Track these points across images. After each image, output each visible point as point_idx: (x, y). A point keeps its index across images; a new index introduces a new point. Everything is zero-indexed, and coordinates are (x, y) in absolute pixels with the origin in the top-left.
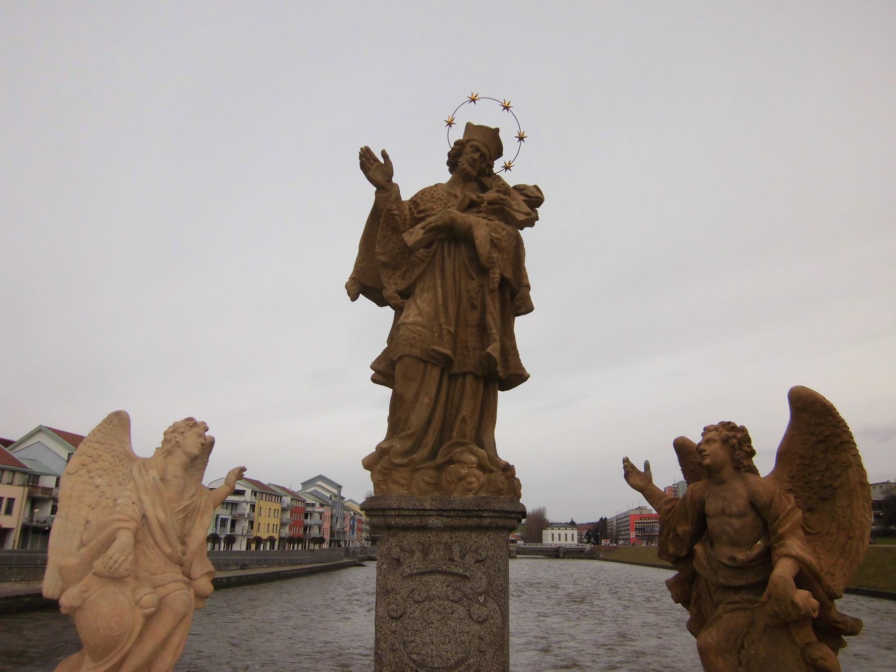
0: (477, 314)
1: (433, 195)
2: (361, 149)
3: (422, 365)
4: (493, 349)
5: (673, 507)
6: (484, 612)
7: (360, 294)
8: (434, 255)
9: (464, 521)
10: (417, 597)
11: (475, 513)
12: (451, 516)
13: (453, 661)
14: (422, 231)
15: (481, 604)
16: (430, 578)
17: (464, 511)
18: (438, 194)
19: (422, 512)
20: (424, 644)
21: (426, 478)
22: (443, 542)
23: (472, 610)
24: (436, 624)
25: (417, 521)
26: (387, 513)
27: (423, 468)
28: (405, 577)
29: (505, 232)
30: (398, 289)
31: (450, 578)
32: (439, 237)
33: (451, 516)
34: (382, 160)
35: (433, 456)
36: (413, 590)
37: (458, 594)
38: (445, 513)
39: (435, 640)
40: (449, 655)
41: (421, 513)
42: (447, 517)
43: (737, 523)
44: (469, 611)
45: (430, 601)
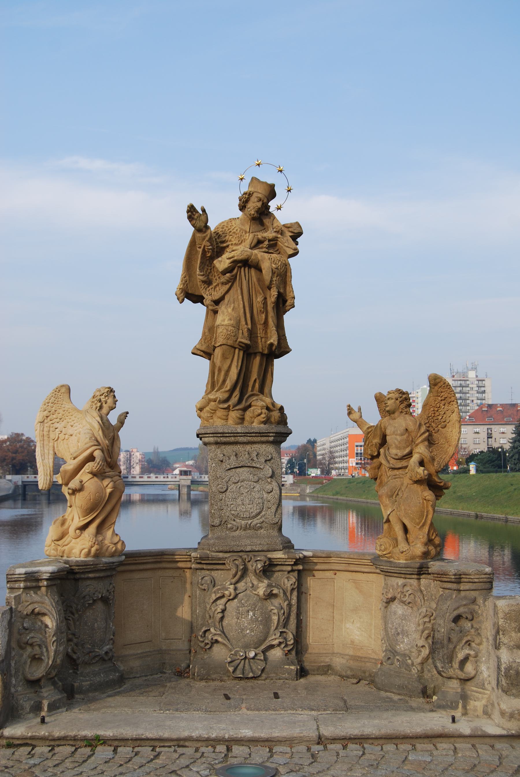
0: (263, 316)
1: (230, 230)
2: (188, 207)
3: (233, 349)
4: (273, 339)
5: (372, 430)
7: (185, 298)
8: (236, 277)
9: (259, 439)
11: (266, 434)
12: (252, 436)
14: (228, 261)
16: (241, 470)
17: (260, 433)
18: (233, 229)
19: (235, 434)
24: (245, 494)
25: (233, 439)
29: (280, 262)
30: (214, 299)
31: (252, 469)
32: (238, 265)
33: (252, 436)
34: (201, 212)
35: (240, 401)
37: (256, 478)
38: (249, 435)
41: (235, 435)
42: (250, 436)
43: (399, 438)
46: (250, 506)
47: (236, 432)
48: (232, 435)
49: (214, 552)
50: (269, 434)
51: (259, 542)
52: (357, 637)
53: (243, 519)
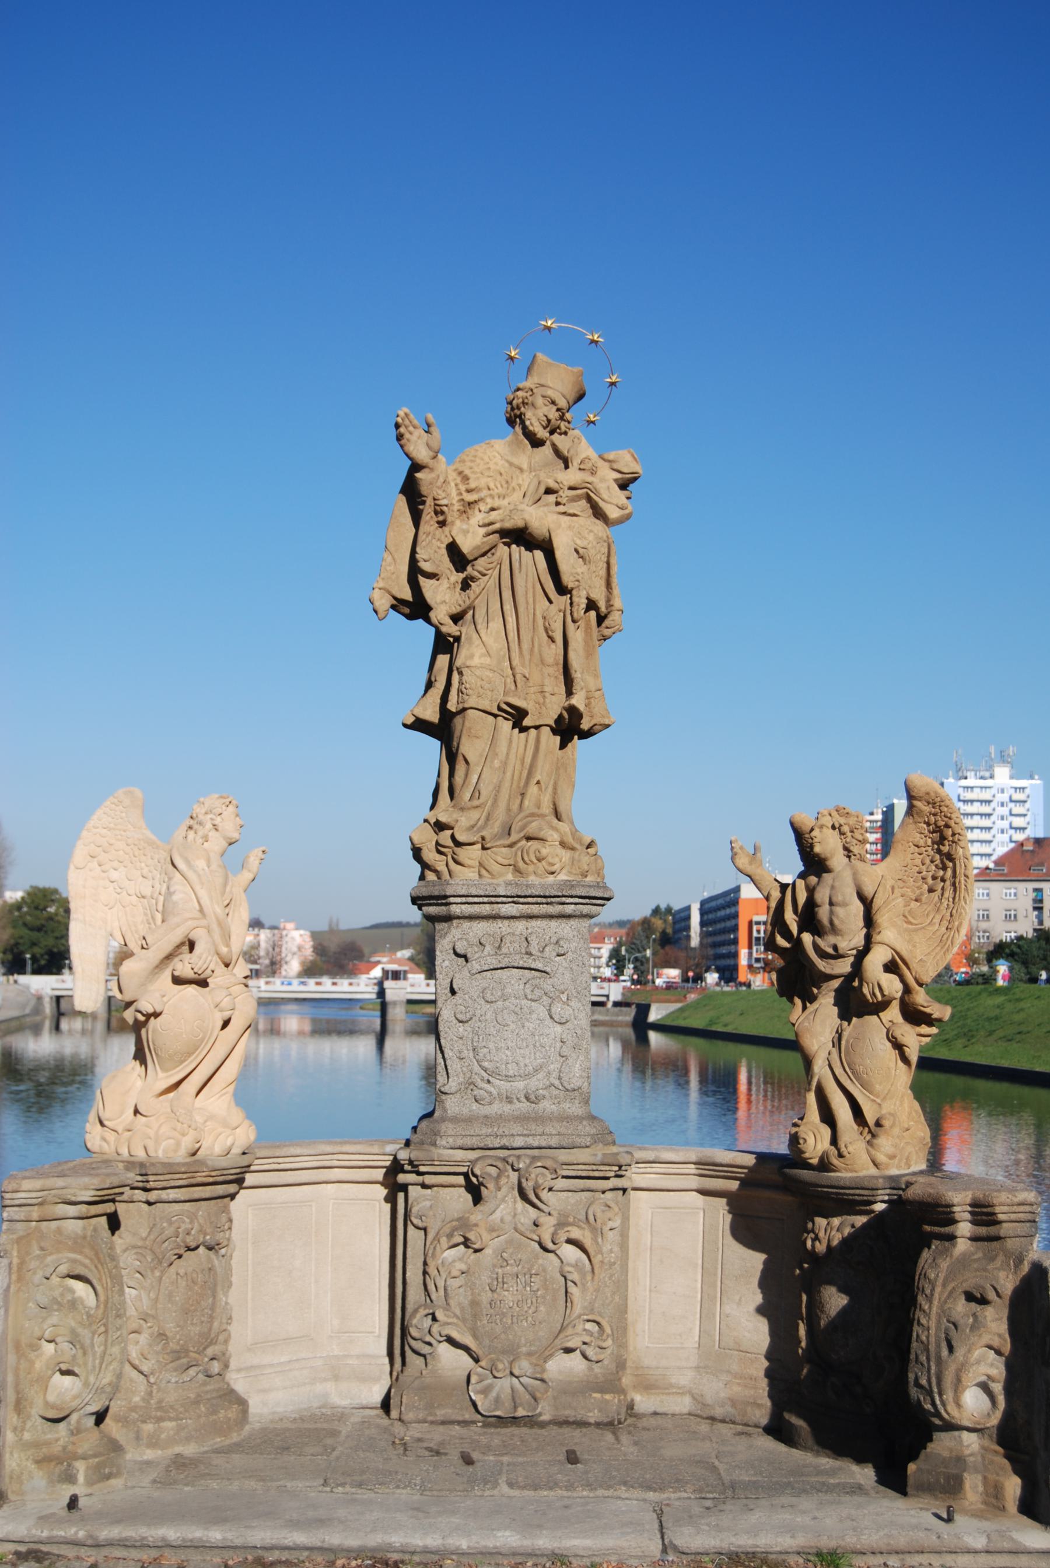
6: (568, 1012)
10: (489, 997)
13: (531, 1068)
15: (564, 1003)
19: (493, 898)
20: (497, 1049)
21: (500, 859)
22: (517, 933)
23: (553, 1010)
24: (512, 1026)
26: (452, 900)
27: (496, 846)
28: (474, 974)
36: (485, 989)
38: (521, 900)
39: (510, 1044)
40: (527, 1061)
41: (493, 899)
44: (549, 1010)
45: (505, 1000)
46: (522, 1051)
47: (494, 894)
48: (486, 900)
49: (445, 1148)
50: (564, 899)
51: (540, 1130)
52: (747, 1334)
53: (508, 1078)
